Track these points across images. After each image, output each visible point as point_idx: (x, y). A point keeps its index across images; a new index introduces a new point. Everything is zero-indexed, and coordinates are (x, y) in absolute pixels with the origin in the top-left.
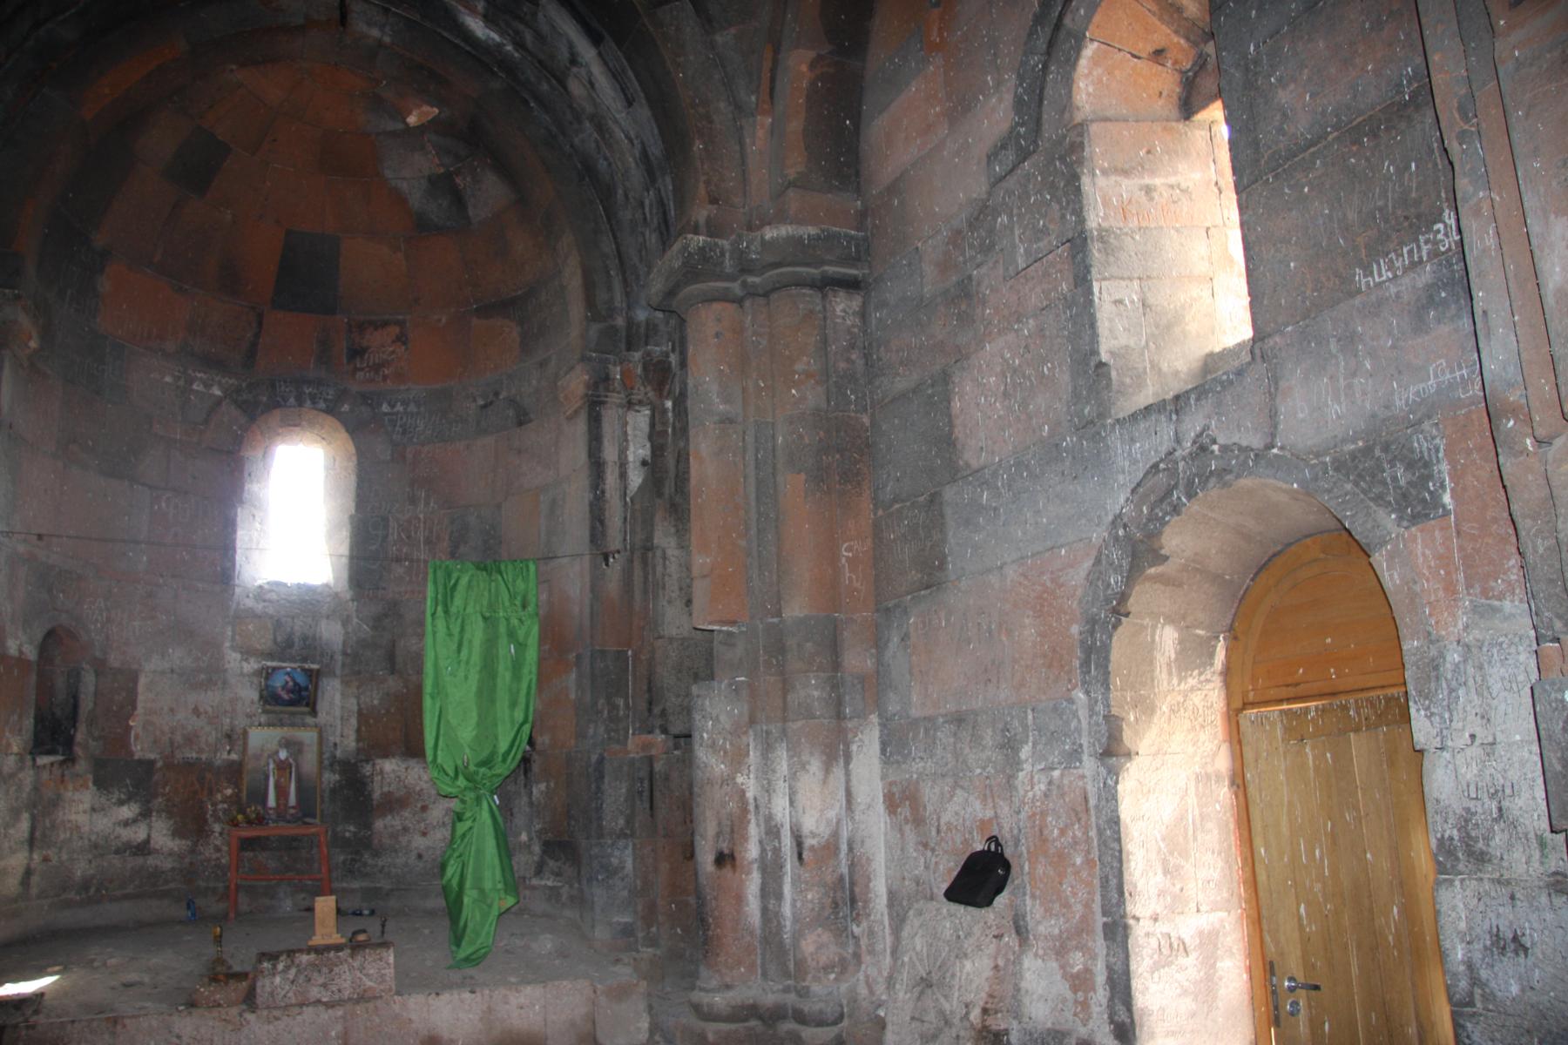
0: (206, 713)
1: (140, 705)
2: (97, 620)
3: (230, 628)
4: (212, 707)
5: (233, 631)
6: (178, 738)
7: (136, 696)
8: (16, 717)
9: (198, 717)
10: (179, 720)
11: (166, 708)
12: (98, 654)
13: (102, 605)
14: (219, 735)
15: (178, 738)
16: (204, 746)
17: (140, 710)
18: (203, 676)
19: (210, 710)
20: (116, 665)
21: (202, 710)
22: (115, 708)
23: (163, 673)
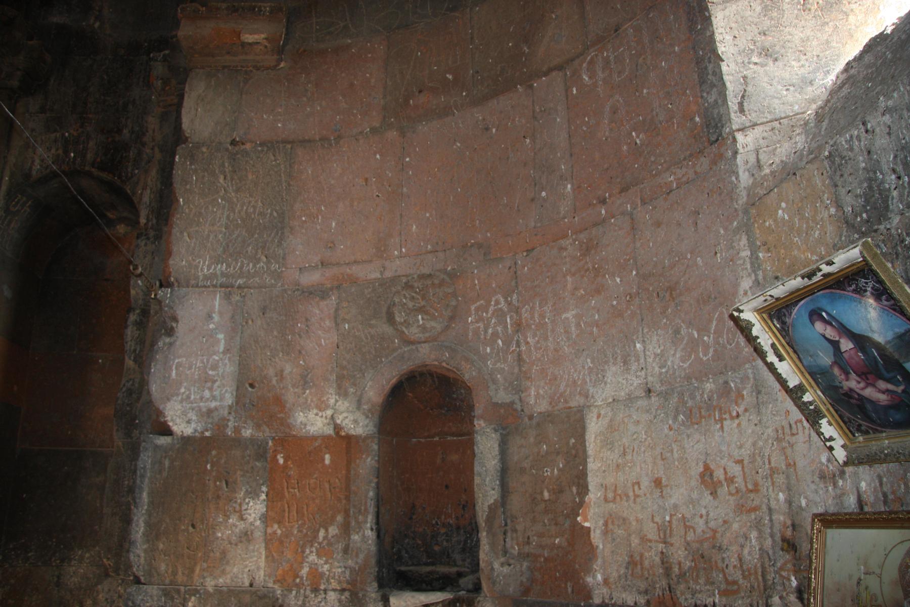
0: (730, 480)
1: (593, 481)
2: (495, 335)
3: (744, 241)
4: (740, 462)
5: (752, 245)
6: (679, 554)
7: (585, 463)
8: (333, 530)
9: (714, 494)
10: (675, 506)
11: (645, 483)
12: (503, 396)
13: (503, 305)
14: (769, 542)
15: (679, 554)
16: (737, 575)
17: (594, 495)
18: (709, 386)
19: (735, 470)
20: (543, 406)
21: (719, 474)
22: (546, 495)
23: (630, 399)
